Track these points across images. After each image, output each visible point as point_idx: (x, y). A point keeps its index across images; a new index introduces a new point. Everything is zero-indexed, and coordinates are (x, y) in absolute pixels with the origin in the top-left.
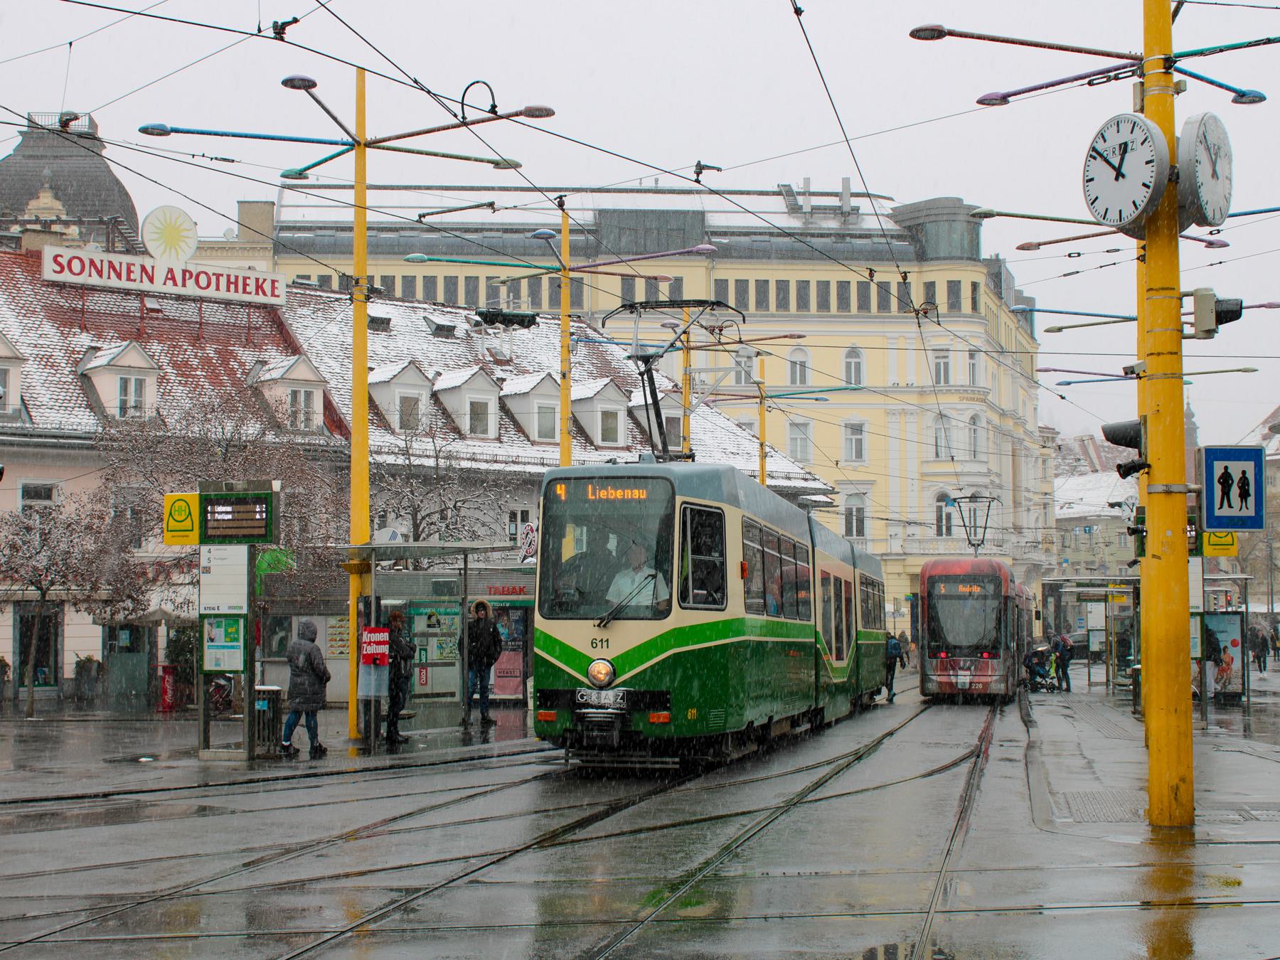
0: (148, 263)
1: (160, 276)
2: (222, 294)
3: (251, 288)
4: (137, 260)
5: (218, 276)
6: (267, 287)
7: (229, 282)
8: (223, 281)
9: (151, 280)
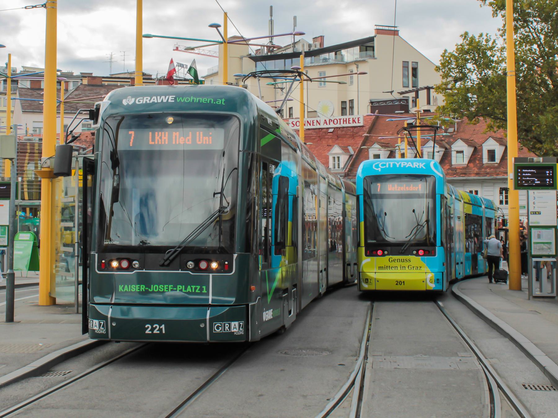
0: (318, 119)
3: (351, 121)
4: (315, 119)
5: (340, 119)
6: (356, 120)
7: (344, 121)
8: (342, 121)
9: (319, 124)
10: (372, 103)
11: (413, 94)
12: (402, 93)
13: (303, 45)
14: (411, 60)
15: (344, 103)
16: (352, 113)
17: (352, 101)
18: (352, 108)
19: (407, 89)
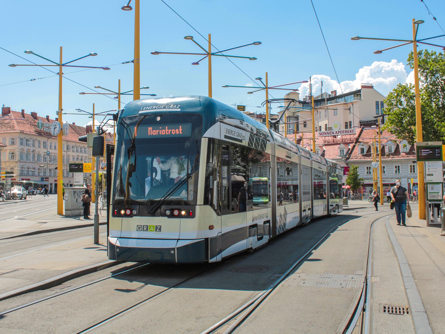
0: (333, 131)
1: (335, 133)
2: (345, 134)
4: (331, 131)
10: (360, 122)
11: (381, 118)
12: (376, 117)
13: (326, 95)
14: (380, 100)
15: (346, 123)
16: (351, 128)
17: (350, 122)
18: (350, 125)
19: (378, 115)
